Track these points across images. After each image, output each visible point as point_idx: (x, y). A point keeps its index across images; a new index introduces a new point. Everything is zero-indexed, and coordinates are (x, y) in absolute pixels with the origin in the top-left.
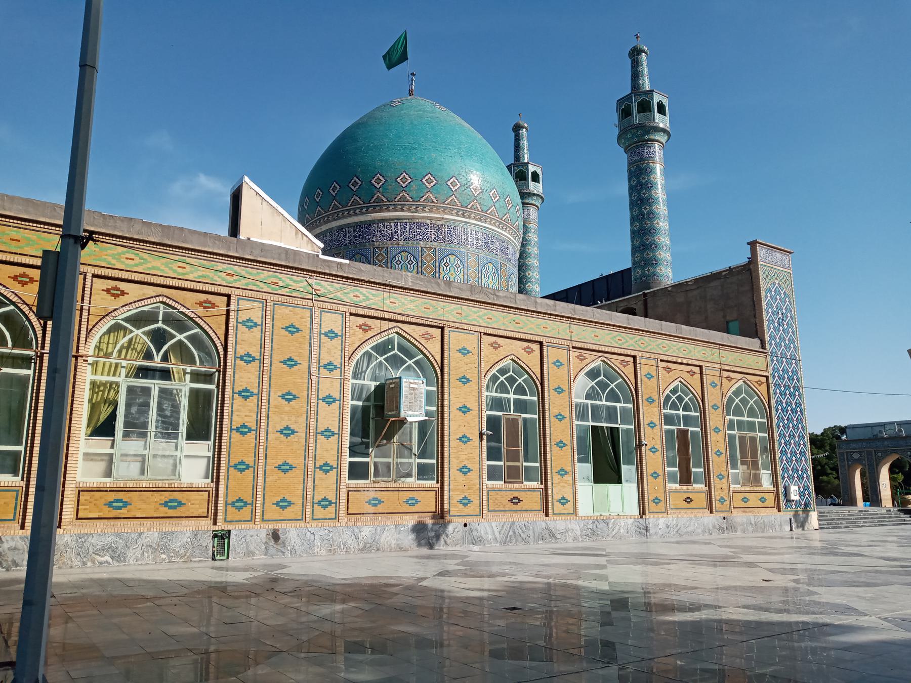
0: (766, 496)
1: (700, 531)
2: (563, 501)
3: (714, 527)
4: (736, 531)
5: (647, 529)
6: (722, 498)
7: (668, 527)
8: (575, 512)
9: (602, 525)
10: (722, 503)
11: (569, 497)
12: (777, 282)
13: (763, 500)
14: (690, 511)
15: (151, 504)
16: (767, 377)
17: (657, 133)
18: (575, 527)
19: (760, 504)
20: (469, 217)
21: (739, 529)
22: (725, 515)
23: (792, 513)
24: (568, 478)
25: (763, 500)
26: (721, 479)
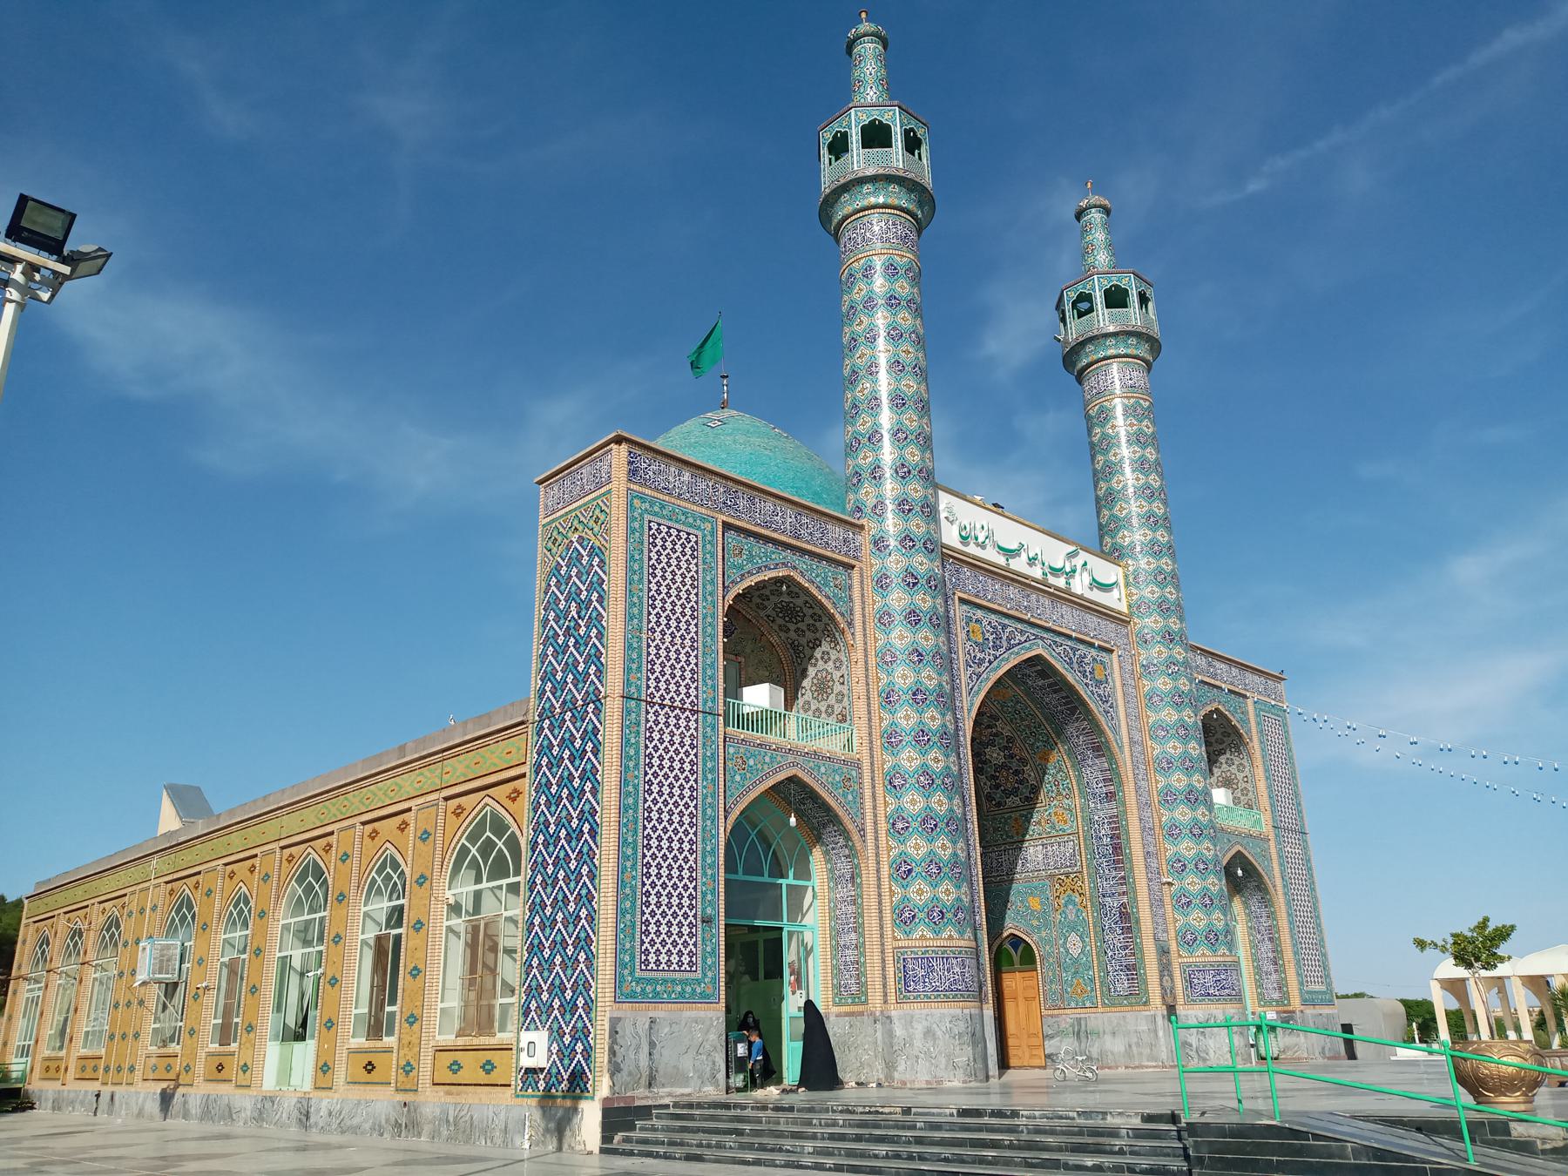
1: (367, 1126)
3: (387, 1121)
4: (419, 1135)
5: (307, 1116)
6: (408, 1064)
9: (268, 1105)
10: (407, 1073)
14: (369, 1087)
16: (523, 776)
17: (838, 206)
18: (244, 1102)
19: (481, 1077)
21: (427, 1129)
22: (408, 1097)
23: (533, 1102)
25: (488, 1067)
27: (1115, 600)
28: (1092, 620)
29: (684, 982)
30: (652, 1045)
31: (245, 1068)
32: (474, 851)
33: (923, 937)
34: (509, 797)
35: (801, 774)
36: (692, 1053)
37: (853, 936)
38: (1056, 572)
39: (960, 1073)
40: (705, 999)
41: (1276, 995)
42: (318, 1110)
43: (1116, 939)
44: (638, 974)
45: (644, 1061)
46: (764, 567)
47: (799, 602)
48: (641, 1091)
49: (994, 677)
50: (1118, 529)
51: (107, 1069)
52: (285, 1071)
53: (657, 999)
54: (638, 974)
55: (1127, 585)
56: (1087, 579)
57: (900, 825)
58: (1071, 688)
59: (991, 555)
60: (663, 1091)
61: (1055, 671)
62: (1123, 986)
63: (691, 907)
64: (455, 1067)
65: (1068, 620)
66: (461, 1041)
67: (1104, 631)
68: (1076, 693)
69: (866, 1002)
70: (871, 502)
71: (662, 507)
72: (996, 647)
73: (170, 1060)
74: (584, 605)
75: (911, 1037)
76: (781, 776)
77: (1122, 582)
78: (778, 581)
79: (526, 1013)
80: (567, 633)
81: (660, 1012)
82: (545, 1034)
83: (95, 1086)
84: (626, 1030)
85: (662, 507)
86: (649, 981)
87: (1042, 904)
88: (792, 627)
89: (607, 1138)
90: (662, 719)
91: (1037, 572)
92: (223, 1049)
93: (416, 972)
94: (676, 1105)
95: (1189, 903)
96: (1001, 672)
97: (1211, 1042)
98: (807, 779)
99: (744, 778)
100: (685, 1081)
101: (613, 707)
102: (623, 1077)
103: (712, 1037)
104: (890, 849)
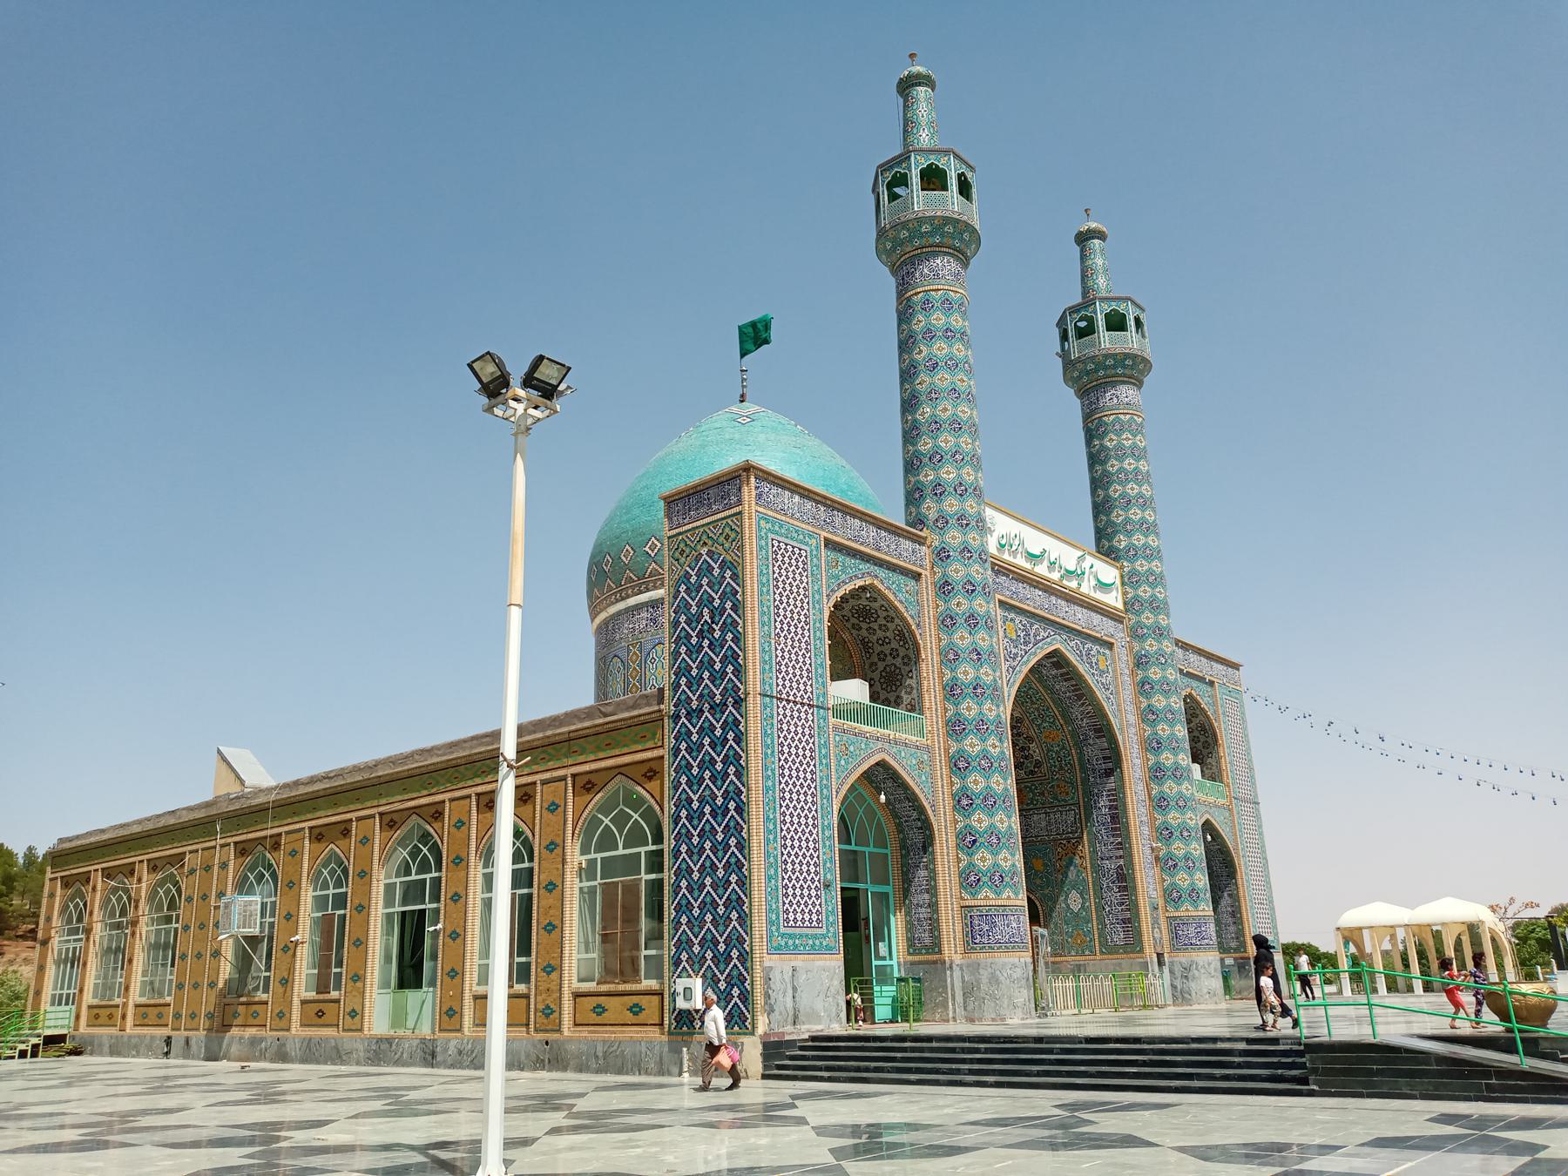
0: (644, 1001)
2: (353, 1014)
3: (528, 1056)
5: (433, 1055)
6: (548, 1007)
7: (460, 1053)
8: (361, 1030)
9: (384, 1046)
10: (547, 1016)
11: (358, 1009)
12: (704, 551)
13: (636, 1010)
15: (152, 1019)
19: (629, 1017)
20: (628, 597)
24: (359, 984)
25: (636, 1010)
26: (549, 973)
27: (1114, 600)
28: (1096, 618)
29: (815, 937)
30: (795, 989)
31: (353, 1014)
32: (607, 821)
33: (986, 898)
34: (644, 775)
35: (888, 758)
36: (822, 996)
37: (926, 896)
38: (1069, 574)
39: (1019, 1012)
40: (829, 950)
41: (1233, 945)
42: (446, 1050)
43: (1114, 896)
44: (782, 930)
45: (790, 1004)
46: (857, 576)
47: (876, 605)
48: (789, 1028)
49: (1026, 669)
50: (1115, 533)
51: (177, 1016)
52: (398, 1017)
53: (795, 951)
54: (782, 930)
55: (1123, 584)
56: (1093, 583)
57: (965, 802)
58: (1080, 677)
59: (1021, 561)
60: (804, 1028)
61: (1068, 663)
62: (1119, 938)
63: (816, 873)
64: (600, 1010)
65: (1079, 618)
66: (604, 988)
67: (1104, 627)
68: (1085, 681)
69: (940, 952)
70: (932, 515)
71: (781, 527)
72: (1026, 643)
73: (113, 1010)
74: (717, 613)
75: (978, 981)
76: (872, 761)
77: (1118, 582)
78: (863, 588)
79: (677, 963)
80: (701, 635)
81: (799, 961)
82: (699, 981)
83: (166, 1032)
84: (776, 976)
85: (781, 527)
86: (790, 936)
87: (1045, 865)
88: (864, 626)
89: (765, 1067)
90: (788, 712)
91: (1055, 576)
92: (321, 997)
93: (550, 928)
94: (813, 1039)
95: (1175, 866)
96: (1030, 665)
97: (1193, 985)
98: (893, 763)
99: (847, 763)
100: (818, 1019)
101: (754, 705)
102: (776, 1016)
103: (836, 982)
104: (956, 822)
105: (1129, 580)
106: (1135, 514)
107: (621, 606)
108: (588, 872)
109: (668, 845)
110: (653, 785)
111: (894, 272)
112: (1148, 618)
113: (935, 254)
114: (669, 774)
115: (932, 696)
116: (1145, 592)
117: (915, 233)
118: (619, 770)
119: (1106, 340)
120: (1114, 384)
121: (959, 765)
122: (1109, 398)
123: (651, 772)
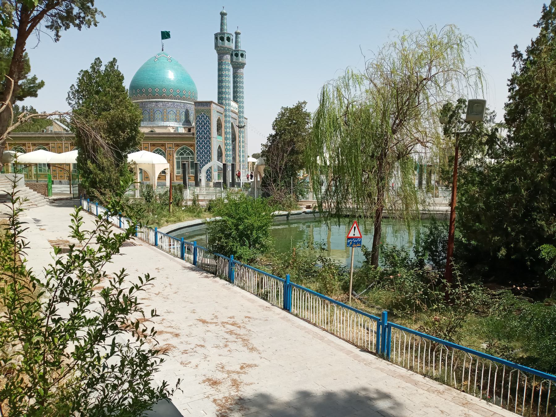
27: (237, 111)
105: (239, 107)
106: (241, 95)
107: (148, 100)
108: (178, 158)
109: (196, 156)
110: (193, 148)
111: (219, 54)
112: (241, 115)
113: (227, 54)
114: (196, 146)
115: (223, 134)
116: (241, 110)
117: (224, 49)
118: (184, 144)
119: (240, 59)
120: (240, 68)
121: (226, 144)
122: (239, 71)
123: (192, 145)
